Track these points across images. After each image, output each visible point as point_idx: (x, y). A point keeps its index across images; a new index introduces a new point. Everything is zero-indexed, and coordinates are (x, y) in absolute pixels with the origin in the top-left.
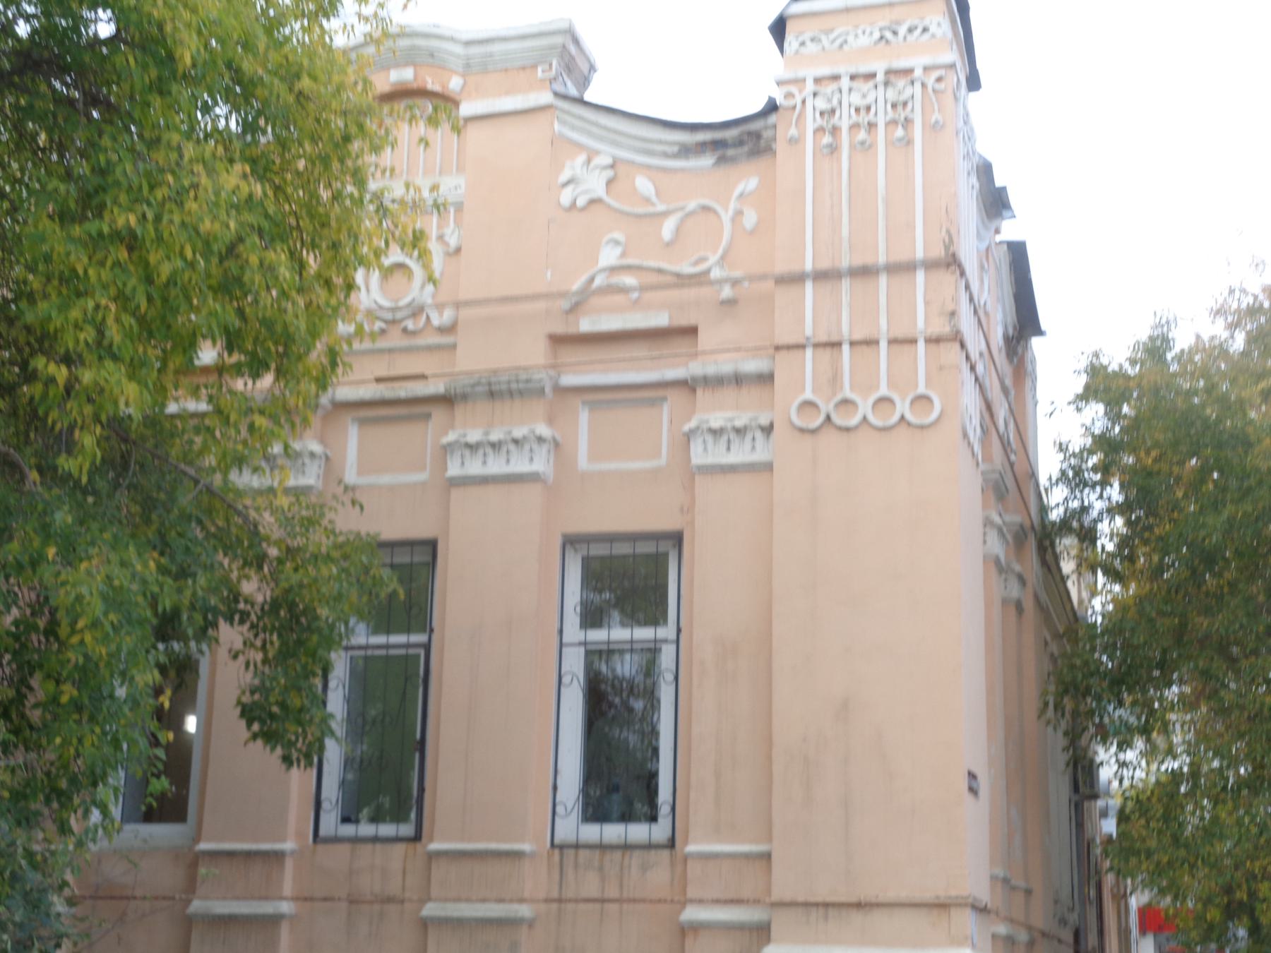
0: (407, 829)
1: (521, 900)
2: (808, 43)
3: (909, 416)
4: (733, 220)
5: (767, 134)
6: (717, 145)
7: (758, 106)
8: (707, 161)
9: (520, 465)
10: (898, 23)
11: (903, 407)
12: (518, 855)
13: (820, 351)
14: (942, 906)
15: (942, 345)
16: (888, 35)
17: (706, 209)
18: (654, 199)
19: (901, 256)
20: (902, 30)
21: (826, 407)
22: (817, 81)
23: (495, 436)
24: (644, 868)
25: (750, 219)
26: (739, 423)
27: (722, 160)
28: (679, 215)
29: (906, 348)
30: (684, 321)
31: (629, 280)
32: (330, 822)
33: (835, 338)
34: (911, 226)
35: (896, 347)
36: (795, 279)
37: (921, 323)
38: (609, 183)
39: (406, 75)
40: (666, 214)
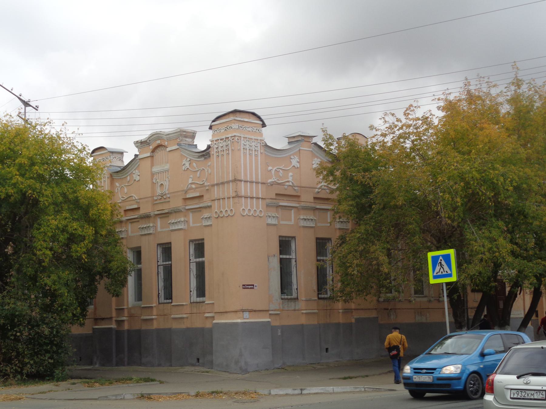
0: (170, 301)
3: (231, 215)
6: (203, 155)
9: (180, 227)
10: (228, 126)
12: (183, 305)
14: (236, 312)
17: (203, 169)
19: (228, 180)
20: (228, 128)
21: (218, 212)
22: (216, 140)
23: (175, 221)
24: (202, 307)
25: (210, 171)
26: (208, 216)
27: (205, 158)
28: (200, 171)
31: (193, 186)
32: (162, 300)
34: (229, 173)
36: (213, 186)
38: (190, 164)
39: (159, 142)
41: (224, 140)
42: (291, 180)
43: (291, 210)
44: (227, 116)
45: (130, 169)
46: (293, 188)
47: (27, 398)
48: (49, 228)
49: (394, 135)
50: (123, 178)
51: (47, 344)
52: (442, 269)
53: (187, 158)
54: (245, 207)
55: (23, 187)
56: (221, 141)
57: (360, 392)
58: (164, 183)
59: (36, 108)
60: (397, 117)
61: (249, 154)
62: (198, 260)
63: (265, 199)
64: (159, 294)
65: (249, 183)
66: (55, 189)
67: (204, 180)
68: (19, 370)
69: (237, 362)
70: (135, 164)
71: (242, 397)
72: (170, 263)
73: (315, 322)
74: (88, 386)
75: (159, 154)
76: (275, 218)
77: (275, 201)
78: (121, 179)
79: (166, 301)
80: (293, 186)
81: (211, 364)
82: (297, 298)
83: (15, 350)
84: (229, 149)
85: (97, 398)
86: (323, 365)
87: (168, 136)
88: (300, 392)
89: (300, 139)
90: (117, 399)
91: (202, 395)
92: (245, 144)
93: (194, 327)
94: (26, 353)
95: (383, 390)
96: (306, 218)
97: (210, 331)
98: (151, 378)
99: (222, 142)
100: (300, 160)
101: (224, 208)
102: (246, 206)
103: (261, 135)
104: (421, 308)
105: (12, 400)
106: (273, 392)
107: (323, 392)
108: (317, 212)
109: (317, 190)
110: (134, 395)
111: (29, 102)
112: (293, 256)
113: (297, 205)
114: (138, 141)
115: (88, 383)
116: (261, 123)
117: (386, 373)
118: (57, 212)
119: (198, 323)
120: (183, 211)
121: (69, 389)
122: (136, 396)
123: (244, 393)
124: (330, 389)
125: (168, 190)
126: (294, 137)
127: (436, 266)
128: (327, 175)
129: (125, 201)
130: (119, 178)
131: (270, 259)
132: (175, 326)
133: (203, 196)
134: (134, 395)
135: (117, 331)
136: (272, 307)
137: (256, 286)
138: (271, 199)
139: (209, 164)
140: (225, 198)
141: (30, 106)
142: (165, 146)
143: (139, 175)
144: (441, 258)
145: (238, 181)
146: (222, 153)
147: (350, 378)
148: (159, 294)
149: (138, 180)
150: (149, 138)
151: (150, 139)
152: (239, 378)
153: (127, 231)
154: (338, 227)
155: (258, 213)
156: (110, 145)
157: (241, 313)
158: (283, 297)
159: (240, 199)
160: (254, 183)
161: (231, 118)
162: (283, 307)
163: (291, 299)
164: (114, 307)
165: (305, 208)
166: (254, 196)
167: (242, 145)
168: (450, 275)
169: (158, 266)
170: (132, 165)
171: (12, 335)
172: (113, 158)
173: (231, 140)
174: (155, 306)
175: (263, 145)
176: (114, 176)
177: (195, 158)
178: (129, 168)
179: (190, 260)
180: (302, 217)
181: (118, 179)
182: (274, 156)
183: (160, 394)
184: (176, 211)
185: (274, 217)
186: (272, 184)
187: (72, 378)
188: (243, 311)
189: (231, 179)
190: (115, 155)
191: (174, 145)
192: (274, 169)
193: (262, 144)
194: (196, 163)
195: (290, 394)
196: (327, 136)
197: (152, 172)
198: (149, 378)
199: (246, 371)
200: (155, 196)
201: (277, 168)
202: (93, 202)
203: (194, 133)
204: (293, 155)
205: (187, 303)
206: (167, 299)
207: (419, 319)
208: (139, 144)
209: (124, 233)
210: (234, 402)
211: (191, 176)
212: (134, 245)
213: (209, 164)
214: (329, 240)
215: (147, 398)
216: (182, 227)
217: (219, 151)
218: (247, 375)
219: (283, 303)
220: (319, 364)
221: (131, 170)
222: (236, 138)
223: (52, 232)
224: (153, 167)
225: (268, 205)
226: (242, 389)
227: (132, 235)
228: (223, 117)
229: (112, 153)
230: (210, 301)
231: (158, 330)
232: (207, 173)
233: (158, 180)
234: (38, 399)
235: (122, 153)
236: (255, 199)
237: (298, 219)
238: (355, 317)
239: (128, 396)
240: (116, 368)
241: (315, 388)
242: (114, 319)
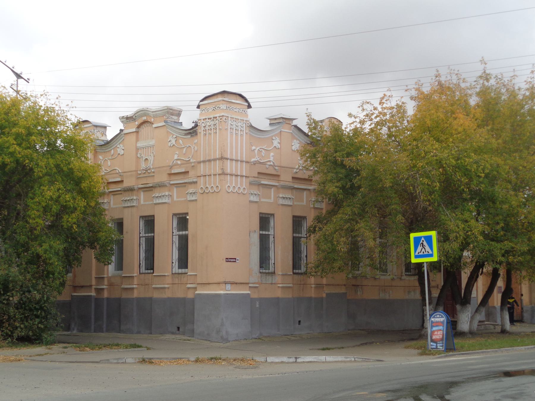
0: (152, 271)
1: (164, 284)
6: (190, 133)
8: (189, 136)
9: (164, 201)
10: (216, 106)
12: (165, 276)
13: (204, 177)
17: (190, 146)
19: (215, 158)
20: (216, 108)
21: (204, 188)
22: (203, 119)
23: (159, 195)
24: (184, 277)
25: (196, 148)
26: (193, 192)
27: (192, 136)
31: (179, 162)
32: (143, 270)
34: (216, 150)
36: (199, 162)
38: (176, 141)
39: (145, 118)
41: (212, 119)
42: (272, 160)
44: (215, 97)
45: (114, 143)
46: (274, 168)
47: (26, 359)
48: (43, 199)
49: (372, 122)
50: (106, 152)
51: (37, 310)
52: (423, 249)
53: (173, 135)
54: (230, 184)
55: (21, 156)
56: (208, 120)
57: (351, 361)
58: (149, 158)
59: (27, 81)
60: (374, 106)
61: (235, 134)
62: (181, 233)
63: (248, 177)
64: (140, 264)
65: (234, 161)
66: (50, 159)
67: (190, 157)
68: (10, 333)
69: (218, 332)
70: (120, 138)
71: (241, 363)
72: (152, 234)
73: (290, 296)
74: (79, 350)
75: (145, 130)
76: (257, 196)
77: (257, 179)
78: (104, 152)
80: (273, 166)
81: (192, 333)
82: (274, 273)
83: (7, 313)
85: (99, 361)
86: (296, 337)
87: (154, 113)
88: (295, 360)
89: (281, 121)
90: (119, 363)
91: (202, 360)
92: (232, 124)
93: (175, 297)
94: (17, 317)
95: (371, 360)
96: (285, 196)
97: (193, 301)
98: (137, 344)
99: (209, 121)
100: (281, 141)
101: (210, 184)
102: (231, 183)
103: (247, 116)
104: (386, 285)
105: (12, 361)
106: (270, 359)
107: (316, 360)
108: (294, 191)
109: (295, 170)
110: (135, 359)
111: (21, 74)
112: (271, 232)
113: (277, 184)
114: (123, 117)
115: (79, 347)
116: (247, 104)
117: (359, 346)
118: (52, 183)
119: (180, 294)
120: (167, 185)
121: (64, 353)
122: (138, 360)
123: (242, 360)
124: (322, 358)
125: (152, 165)
126: (276, 119)
127: (418, 247)
128: (310, 157)
129: (108, 173)
130: (103, 151)
131: (251, 235)
132: (156, 295)
133: (188, 172)
134: (135, 359)
135: (97, 300)
136: (252, 280)
137: (238, 260)
138: (254, 177)
139: (196, 141)
141: (22, 78)
142: (150, 123)
143: (123, 150)
144: (423, 239)
146: (210, 132)
147: (328, 349)
148: (140, 264)
150: (135, 114)
151: (136, 115)
152: (221, 347)
153: (109, 203)
156: (95, 119)
157: (224, 285)
158: (261, 271)
160: (239, 162)
161: (220, 98)
162: (261, 281)
163: (269, 273)
164: (94, 275)
165: (285, 187)
166: (239, 174)
167: (229, 124)
168: (431, 255)
171: (4, 300)
173: (219, 119)
174: (136, 276)
175: (248, 125)
177: (181, 135)
179: (173, 233)
180: (281, 196)
181: (101, 152)
182: (257, 136)
183: (161, 359)
184: (161, 186)
185: (255, 194)
186: (255, 163)
187: (60, 342)
188: (226, 283)
189: (217, 157)
190: (99, 129)
191: (160, 122)
192: (257, 149)
193: (247, 125)
194: (182, 141)
195: (285, 362)
196: (311, 121)
197: (136, 147)
198: (135, 345)
199: (227, 341)
200: (140, 170)
201: (260, 148)
202: (87, 174)
203: (180, 111)
204: (275, 136)
205: (169, 274)
206: (148, 269)
207: (382, 296)
208: (125, 119)
209: (106, 205)
210: (235, 368)
211: (177, 153)
212: (117, 216)
214: (304, 218)
215: (149, 362)
216: (166, 201)
217: (206, 130)
218: (228, 344)
219: (261, 275)
220: (293, 336)
221: (115, 144)
222: (224, 118)
223: (46, 202)
224: (138, 142)
225: (251, 183)
226: (240, 357)
227: (114, 207)
228: (211, 98)
229: (96, 126)
231: (139, 300)
232: (193, 150)
233: (142, 155)
234: (38, 361)
235: (105, 127)
236: (239, 177)
237: (277, 197)
238: (326, 292)
239: (129, 360)
240: (95, 334)
241: (309, 357)
242: (94, 287)
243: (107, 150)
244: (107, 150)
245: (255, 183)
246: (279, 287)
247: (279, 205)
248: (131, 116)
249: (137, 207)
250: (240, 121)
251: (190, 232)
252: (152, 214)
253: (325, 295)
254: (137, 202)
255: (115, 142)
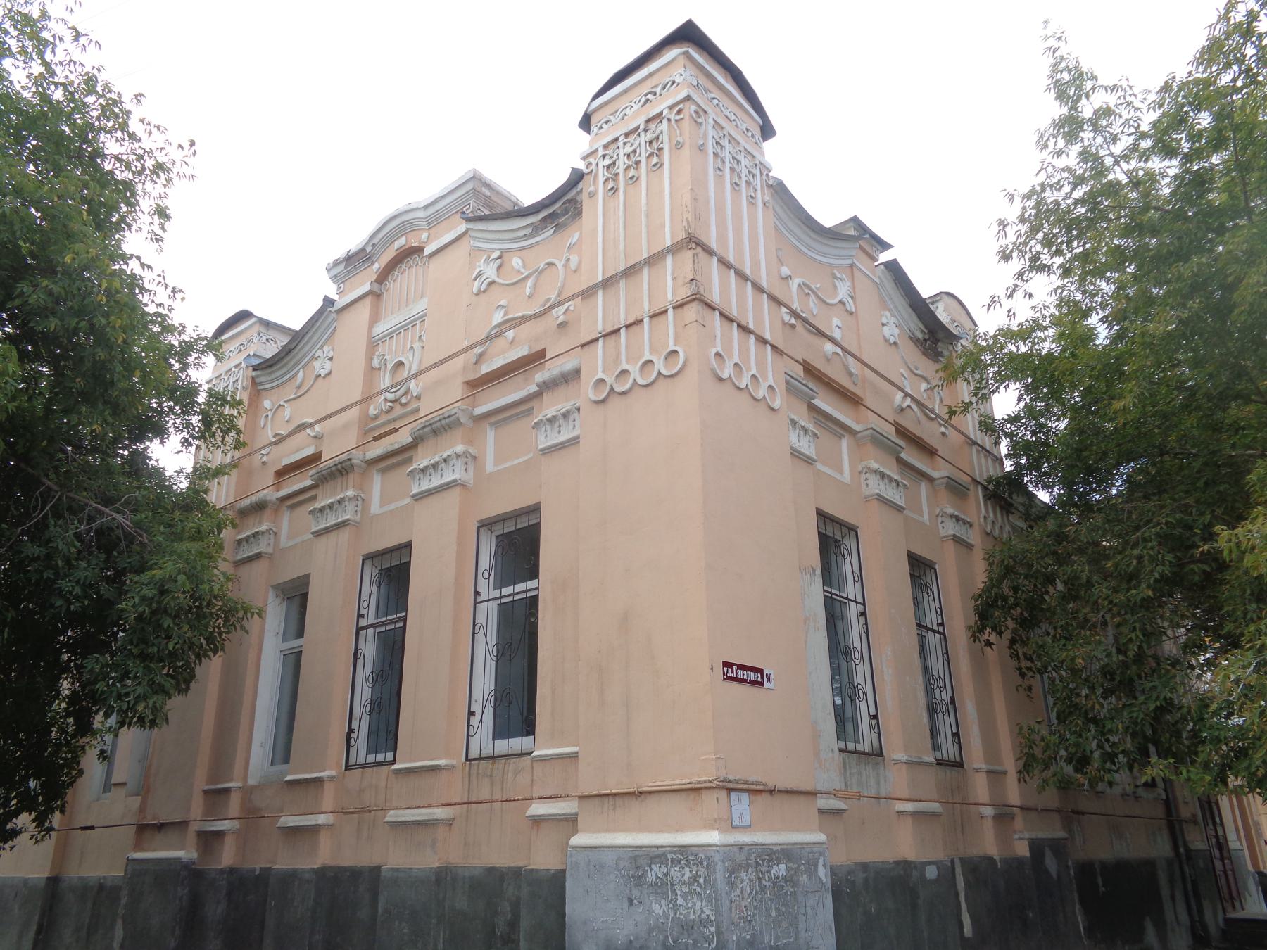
0: (390, 756)
1: (430, 806)
2: (604, 126)
3: (664, 372)
4: (565, 266)
5: (578, 199)
7: (562, 178)
9: (448, 477)
10: (656, 86)
11: (659, 365)
13: (608, 338)
14: (695, 790)
15: (686, 307)
16: (650, 96)
17: (550, 264)
18: (522, 270)
20: (658, 90)
21: (610, 380)
23: (437, 459)
24: (516, 773)
25: (574, 259)
27: (558, 227)
29: (663, 317)
30: (538, 348)
32: (360, 754)
33: (616, 327)
34: (663, 226)
35: (655, 320)
36: (588, 293)
37: (670, 297)
38: (499, 268)
40: (527, 277)
43: (840, 437)
45: (307, 349)
56: (626, 140)
58: (407, 358)
64: (351, 731)
70: (323, 327)
78: (278, 386)
79: (371, 758)
82: (880, 754)
84: (660, 149)
99: (631, 139)
139: (576, 236)
140: (642, 320)
143: (331, 359)
145: (703, 249)
146: (632, 173)
148: (351, 731)
149: (327, 371)
150: (372, 237)
151: (375, 241)
153: (275, 533)
154: (951, 532)
155: (762, 392)
157: (724, 793)
159: (707, 312)
164: (200, 782)
165: (878, 440)
169: (359, 629)
170: (317, 330)
172: (267, 340)
174: (331, 778)
176: (261, 383)
178: (308, 342)
179: (477, 593)
184: (439, 428)
188: (730, 790)
194: (520, 257)
205: (454, 762)
208: (342, 267)
212: (290, 573)
213: (575, 240)
216: (456, 476)
227: (290, 543)
230: (554, 747)
237: (860, 473)
242: (194, 827)
243: (285, 379)
244: (285, 379)
245: (801, 391)
246: (901, 813)
247: (867, 499)
248: (361, 246)
249: (358, 526)
250: (742, 149)
251: (546, 584)
252: (405, 540)
253: (1028, 848)
254: (359, 509)
255: (310, 345)
